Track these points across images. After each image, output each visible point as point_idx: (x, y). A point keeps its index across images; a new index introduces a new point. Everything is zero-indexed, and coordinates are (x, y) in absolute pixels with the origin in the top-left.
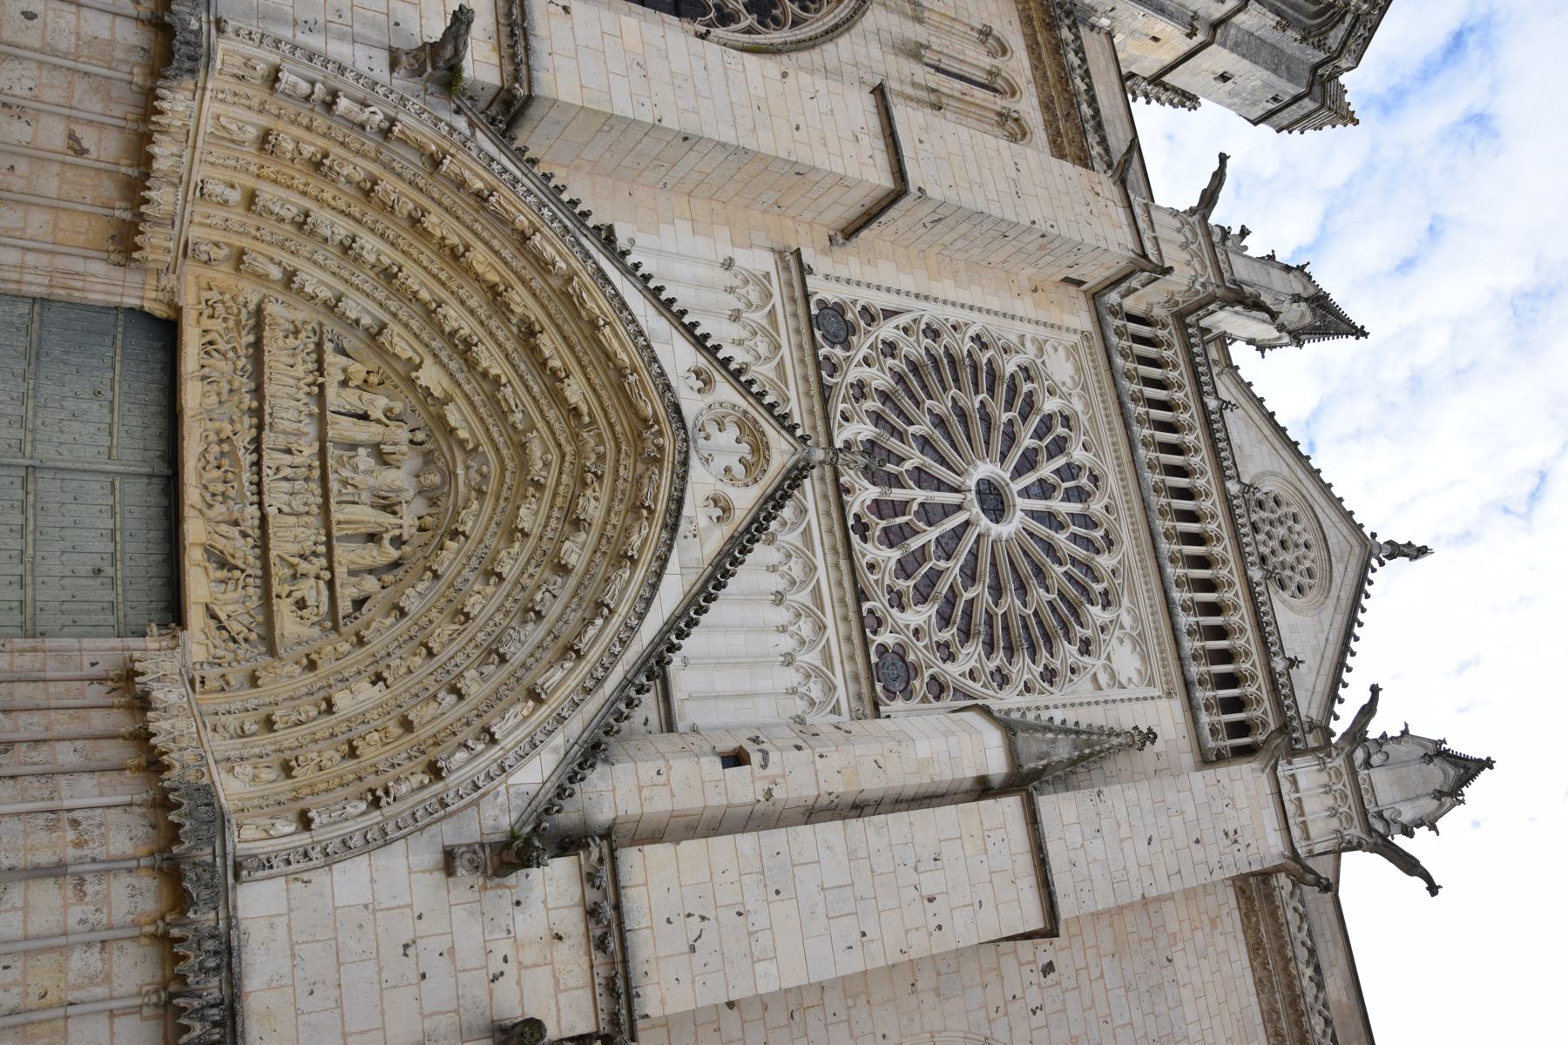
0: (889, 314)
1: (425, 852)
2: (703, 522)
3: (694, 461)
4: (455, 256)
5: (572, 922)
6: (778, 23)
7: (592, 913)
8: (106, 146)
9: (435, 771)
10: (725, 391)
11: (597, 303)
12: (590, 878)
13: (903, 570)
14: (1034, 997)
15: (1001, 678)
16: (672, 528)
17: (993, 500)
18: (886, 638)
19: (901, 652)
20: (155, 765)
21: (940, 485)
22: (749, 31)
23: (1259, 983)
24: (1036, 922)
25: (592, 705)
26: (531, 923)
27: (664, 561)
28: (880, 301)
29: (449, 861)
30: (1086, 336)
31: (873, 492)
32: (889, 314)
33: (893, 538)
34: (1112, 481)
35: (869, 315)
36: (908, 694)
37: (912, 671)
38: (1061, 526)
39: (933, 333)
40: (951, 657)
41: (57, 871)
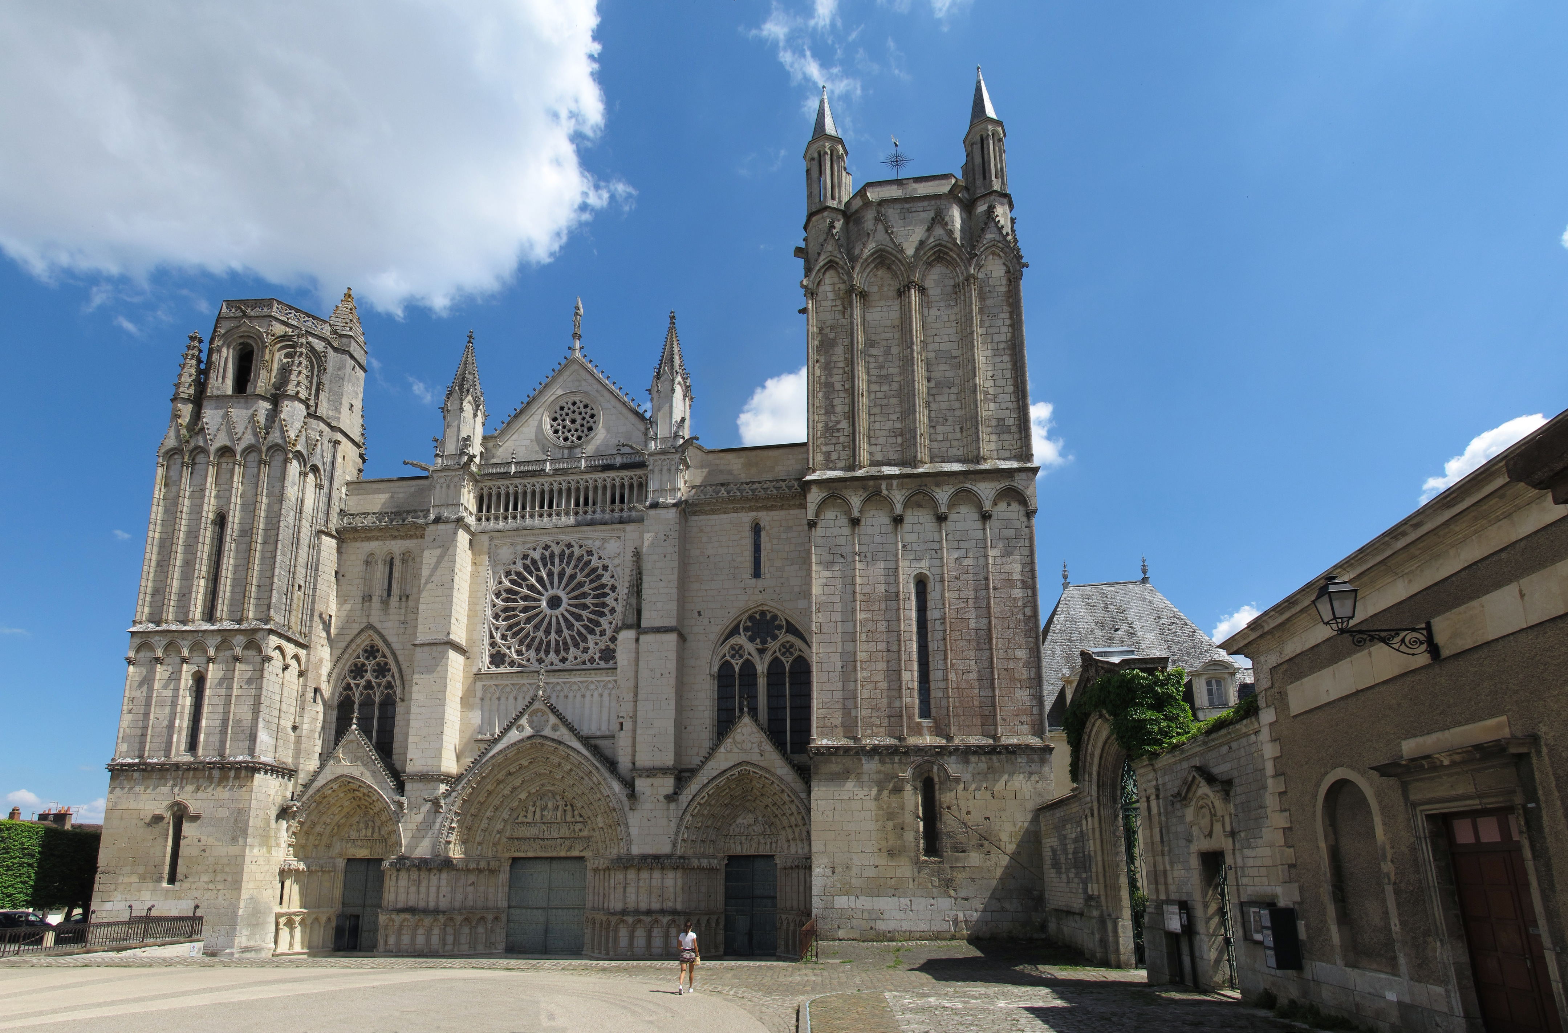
0: (492, 636)
1: (630, 814)
2: (558, 733)
3: (543, 733)
4: (490, 793)
5: (650, 781)
6: (386, 664)
7: (648, 776)
8: (472, 878)
9: (614, 810)
10: (524, 721)
11: (501, 758)
12: (640, 776)
13: (576, 645)
14: (706, 621)
15: (613, 611)
16: (560, 742)
17: (554, 602)
18: (597, 656)
19: (601, 651)
20: (608, 869)
21: (550, 624)
22: (393, 676)
23: (725, 513)
24: (672, 637)
25: (603, 770)
26: (648, 791)
27: (569, 747)
28: (487, 641)
29: (631, 809)
30: (491, 539)
31: (552, 654)
32: (492, 636)
33: (567, 650)
34: (547, 540)
35: (493, 644)
36: (614, 651)
37: (608, 648)
38: (563, 569)
39: (496, 617)
40: (605, 630)
41: (625, 888)
